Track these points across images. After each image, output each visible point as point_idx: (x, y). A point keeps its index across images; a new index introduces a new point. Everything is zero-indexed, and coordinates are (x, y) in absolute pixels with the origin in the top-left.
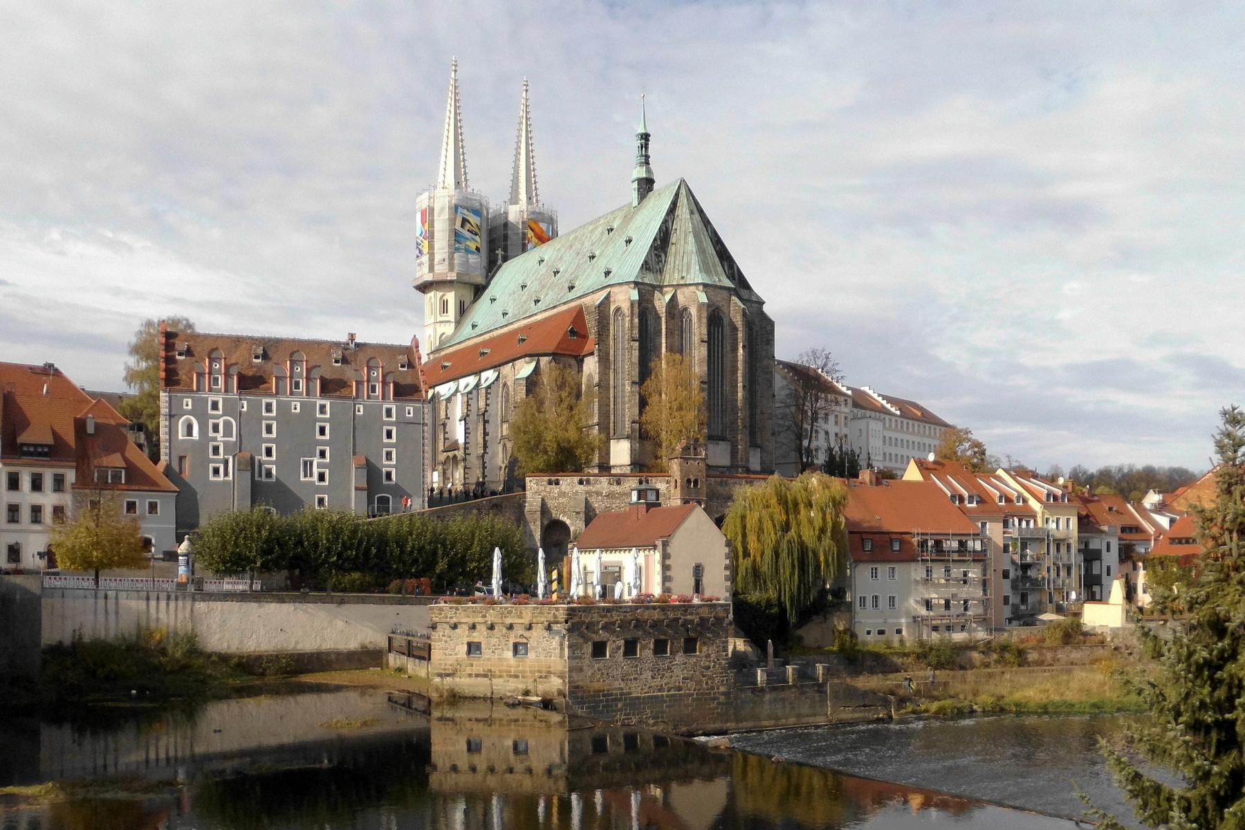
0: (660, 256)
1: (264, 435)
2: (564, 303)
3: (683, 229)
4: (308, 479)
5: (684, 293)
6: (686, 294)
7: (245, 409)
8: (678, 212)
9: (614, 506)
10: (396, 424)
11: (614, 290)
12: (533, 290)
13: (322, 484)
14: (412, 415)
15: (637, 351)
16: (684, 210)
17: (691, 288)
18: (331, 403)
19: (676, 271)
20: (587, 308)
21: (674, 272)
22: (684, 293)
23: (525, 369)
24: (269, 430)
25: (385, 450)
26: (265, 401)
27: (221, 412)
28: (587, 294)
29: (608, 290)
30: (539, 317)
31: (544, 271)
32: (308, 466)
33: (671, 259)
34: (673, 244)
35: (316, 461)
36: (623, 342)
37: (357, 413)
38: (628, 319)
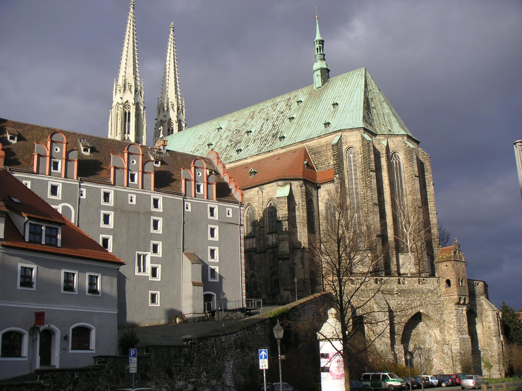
0: (369, 115)
1: (102, 225)
2: (282, 148)
3: (377, 99)
4: (142, 274)
5: (393, 141)
6: (395, 141)
7: (84, 197)
8: (370, 88)
9: (403, 303)
10: (219, 223)
11: (345, 134)
12: (224, 146)
13: (154, 279)
14: (231, 216)
15: (375, 180)
16: (374, 87)
17: (399, 138)
18: (163, 197)
19: (383, 126)
20: (311, 149)
21: (381, 126)
22: (393, 141)
23: (283, 191)
24: (106, 221)
25: (210, 248)
26: (104, 189)
27: (60, 198)
28: (313, 139)
29: (340, 134)
30: (250, 160)
31: (229, 134)
32: (141, 260)
33: (375, 118)
34: (373, 108)
35: (149, 255)
36: (356, 174)
37: (186, 210)
38: (360, 156)
